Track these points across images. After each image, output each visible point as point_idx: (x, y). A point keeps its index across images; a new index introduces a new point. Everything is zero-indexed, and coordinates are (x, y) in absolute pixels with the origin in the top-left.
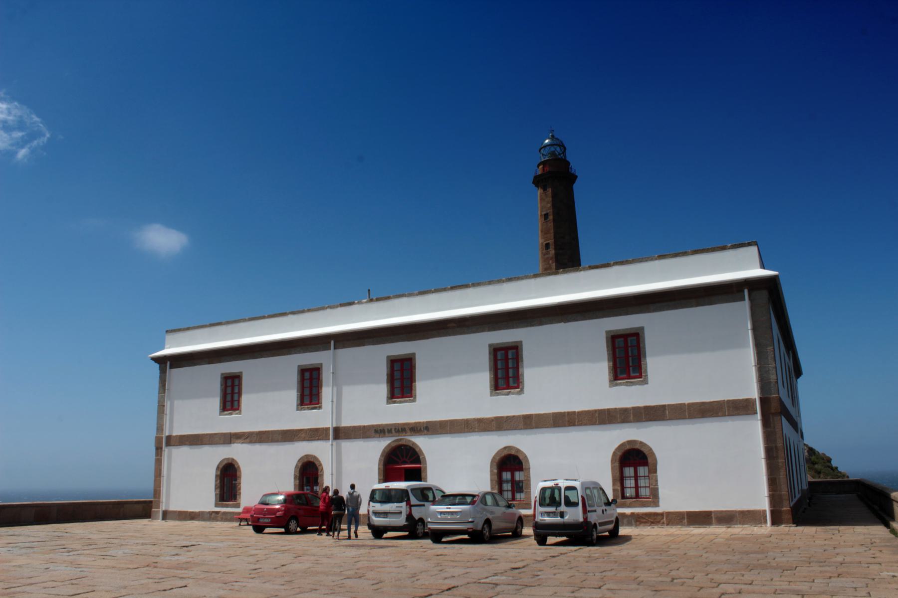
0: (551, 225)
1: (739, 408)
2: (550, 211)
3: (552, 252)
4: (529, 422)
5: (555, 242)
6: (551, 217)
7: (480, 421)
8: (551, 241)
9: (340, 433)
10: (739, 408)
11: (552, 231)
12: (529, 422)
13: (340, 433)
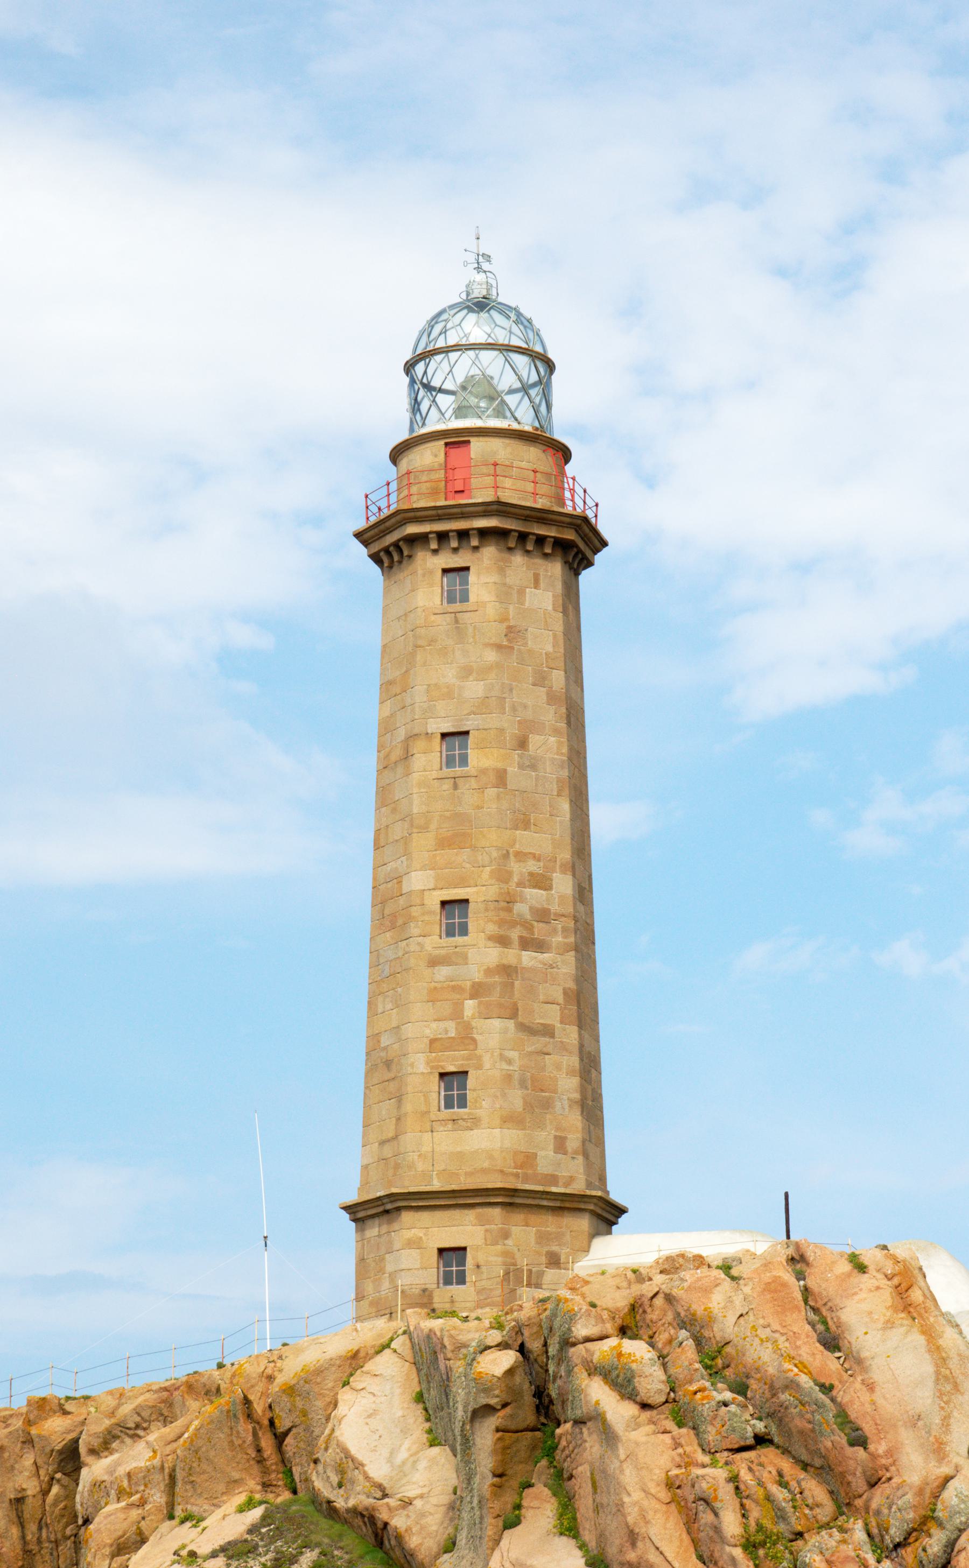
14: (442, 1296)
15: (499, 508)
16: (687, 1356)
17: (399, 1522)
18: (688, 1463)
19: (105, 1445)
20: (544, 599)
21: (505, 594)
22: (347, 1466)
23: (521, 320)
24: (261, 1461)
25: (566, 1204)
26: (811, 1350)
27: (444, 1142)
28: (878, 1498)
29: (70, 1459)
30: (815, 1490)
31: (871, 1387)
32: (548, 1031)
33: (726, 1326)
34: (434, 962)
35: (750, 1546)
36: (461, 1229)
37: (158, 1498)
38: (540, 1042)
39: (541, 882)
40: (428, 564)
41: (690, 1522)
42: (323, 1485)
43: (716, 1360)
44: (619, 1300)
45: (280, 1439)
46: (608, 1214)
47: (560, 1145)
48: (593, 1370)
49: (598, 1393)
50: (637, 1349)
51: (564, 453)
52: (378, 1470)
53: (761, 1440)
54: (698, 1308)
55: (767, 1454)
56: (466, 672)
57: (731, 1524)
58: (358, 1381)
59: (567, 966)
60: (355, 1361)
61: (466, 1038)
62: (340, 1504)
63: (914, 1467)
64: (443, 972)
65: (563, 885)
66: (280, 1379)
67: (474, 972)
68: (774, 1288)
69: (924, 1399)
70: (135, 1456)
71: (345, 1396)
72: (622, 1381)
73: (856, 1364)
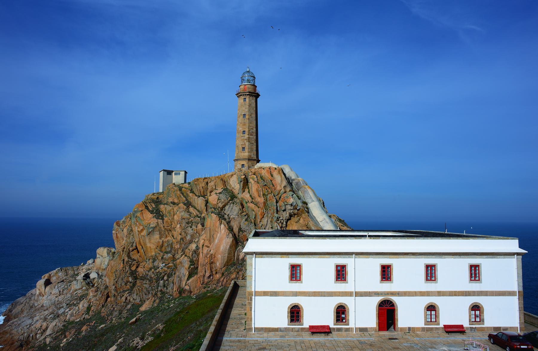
0: (247, 121)
1: (511, 294)
2: (247, 114)
3: (246, 136)
4: (440, 294)
5: (249, 131)
7: (420, 292)
8: (247, 130)
10: (511, 294)
11: (247, 125)
12: (440, 294)
15: (249, 92)
16: (259, 178)
20: (254, 101)
21: (249, 101)
27: (243, 154)
33: (263, 174)
36: (244, 162)
39: (252, 129)
40: (242, 97)
42: (228, 187)
46: (258, 161)
50: (255, 176)
52: (233, 186)
57: (262, 194)
59: (255, 137)
61: (245, 144)
63: (278, 188)
65: (255, 129)
67: (246, 138)
68: (268, 171)
69: (280, 182)
73: (274, 178)
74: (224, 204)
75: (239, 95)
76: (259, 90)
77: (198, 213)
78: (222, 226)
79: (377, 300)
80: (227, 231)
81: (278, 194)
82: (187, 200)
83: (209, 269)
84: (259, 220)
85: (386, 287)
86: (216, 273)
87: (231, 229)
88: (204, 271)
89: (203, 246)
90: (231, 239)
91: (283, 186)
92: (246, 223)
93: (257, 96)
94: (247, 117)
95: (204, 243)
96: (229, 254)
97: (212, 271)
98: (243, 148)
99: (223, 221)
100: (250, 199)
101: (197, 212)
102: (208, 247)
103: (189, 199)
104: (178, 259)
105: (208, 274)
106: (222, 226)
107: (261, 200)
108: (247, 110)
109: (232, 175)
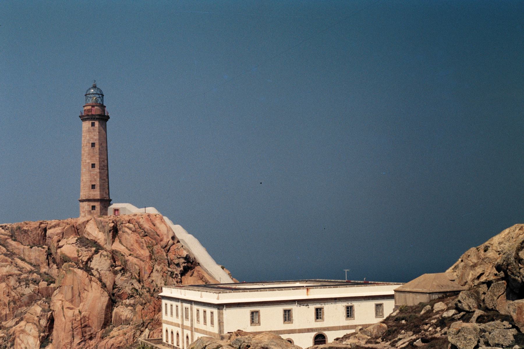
3: (97, 170)
5: (100, 164)
6: (97, 146)
9: (301, 331)
13: (301, 331)
14: (92, 211)
16: (137, 226)
17: (98, 241)
18: (138, 238)
19: (50, 228)
22: (89, 234)
23: (101, 91)
24: (75, 232)
25: (106, 201)
26: (152, 226)
28: (162, 243)
29: (45, 230)
30: (154, 241)
31: (160, 231)
32: (104, 180)
33: (141, 223)
34: (91, 171)
35: (147, 247)
37: (61, 236)
38: (103, 181)
41: (139, 244)
43: (141, 227)
44: (127, 219)
45: (78, 230)
47: (106, 193)
48: (125, 227)
49: (127, 230)
50: (131, 226)
51: (105, 107)
53: (146, 236)
54: (138, 221)
55: (147, 237)
56: (94, 135)
57: (145, 245)
58: (88, 223)
60: (88, 221)
61: (95, 180)
62: (89, 238)
63: (165, 240)
64: (92, 173)
65: (106, 161)
66: (78, 223)
68: (147, 219)
69: (166, 232)
70: (58, 230)
71: (87, 226)
72: (130, 229)
74: (88, 257)
75: (84, 118)
76: (109, 111)
77: (33, 268)
78: (94, 284)
79: (313, 334)
80: (101, 289)
81: (166, 246)
82: (8, 250)
83: (80, 334)
84: (146, 276)
85: (319, 325)
86: (91, 338)
87: (104, 286)
88: (70, 338)
89: (63, 308)
90: (108, 298)
91: (170, 237)
92: (124, 278)
93: (103, 119)
94: (97, 146)
95: (62, 304)
96: (106, 315)
97: (83, 336)
98: (93, 187)
99: (93, 278)
100: (127, 252)
101: (30, 266)
102: (71, 309)
103: (10, 248)
104: (11, 327)
105: (77, 340)
106: (94, 284)
107: (145, 253)
108: (97, 137)
109: (88, 221)
